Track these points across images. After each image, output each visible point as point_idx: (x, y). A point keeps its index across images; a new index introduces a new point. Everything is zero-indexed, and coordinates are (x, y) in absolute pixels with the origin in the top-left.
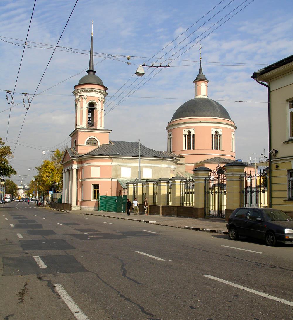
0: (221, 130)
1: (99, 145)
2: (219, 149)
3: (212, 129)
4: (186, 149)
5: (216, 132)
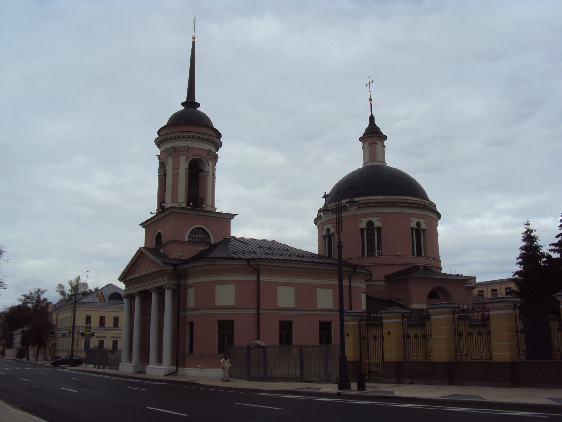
0: (424, 220)
1: (213, 241)
3: (411, 219)
4: (366, 255)
5: (418, 224)
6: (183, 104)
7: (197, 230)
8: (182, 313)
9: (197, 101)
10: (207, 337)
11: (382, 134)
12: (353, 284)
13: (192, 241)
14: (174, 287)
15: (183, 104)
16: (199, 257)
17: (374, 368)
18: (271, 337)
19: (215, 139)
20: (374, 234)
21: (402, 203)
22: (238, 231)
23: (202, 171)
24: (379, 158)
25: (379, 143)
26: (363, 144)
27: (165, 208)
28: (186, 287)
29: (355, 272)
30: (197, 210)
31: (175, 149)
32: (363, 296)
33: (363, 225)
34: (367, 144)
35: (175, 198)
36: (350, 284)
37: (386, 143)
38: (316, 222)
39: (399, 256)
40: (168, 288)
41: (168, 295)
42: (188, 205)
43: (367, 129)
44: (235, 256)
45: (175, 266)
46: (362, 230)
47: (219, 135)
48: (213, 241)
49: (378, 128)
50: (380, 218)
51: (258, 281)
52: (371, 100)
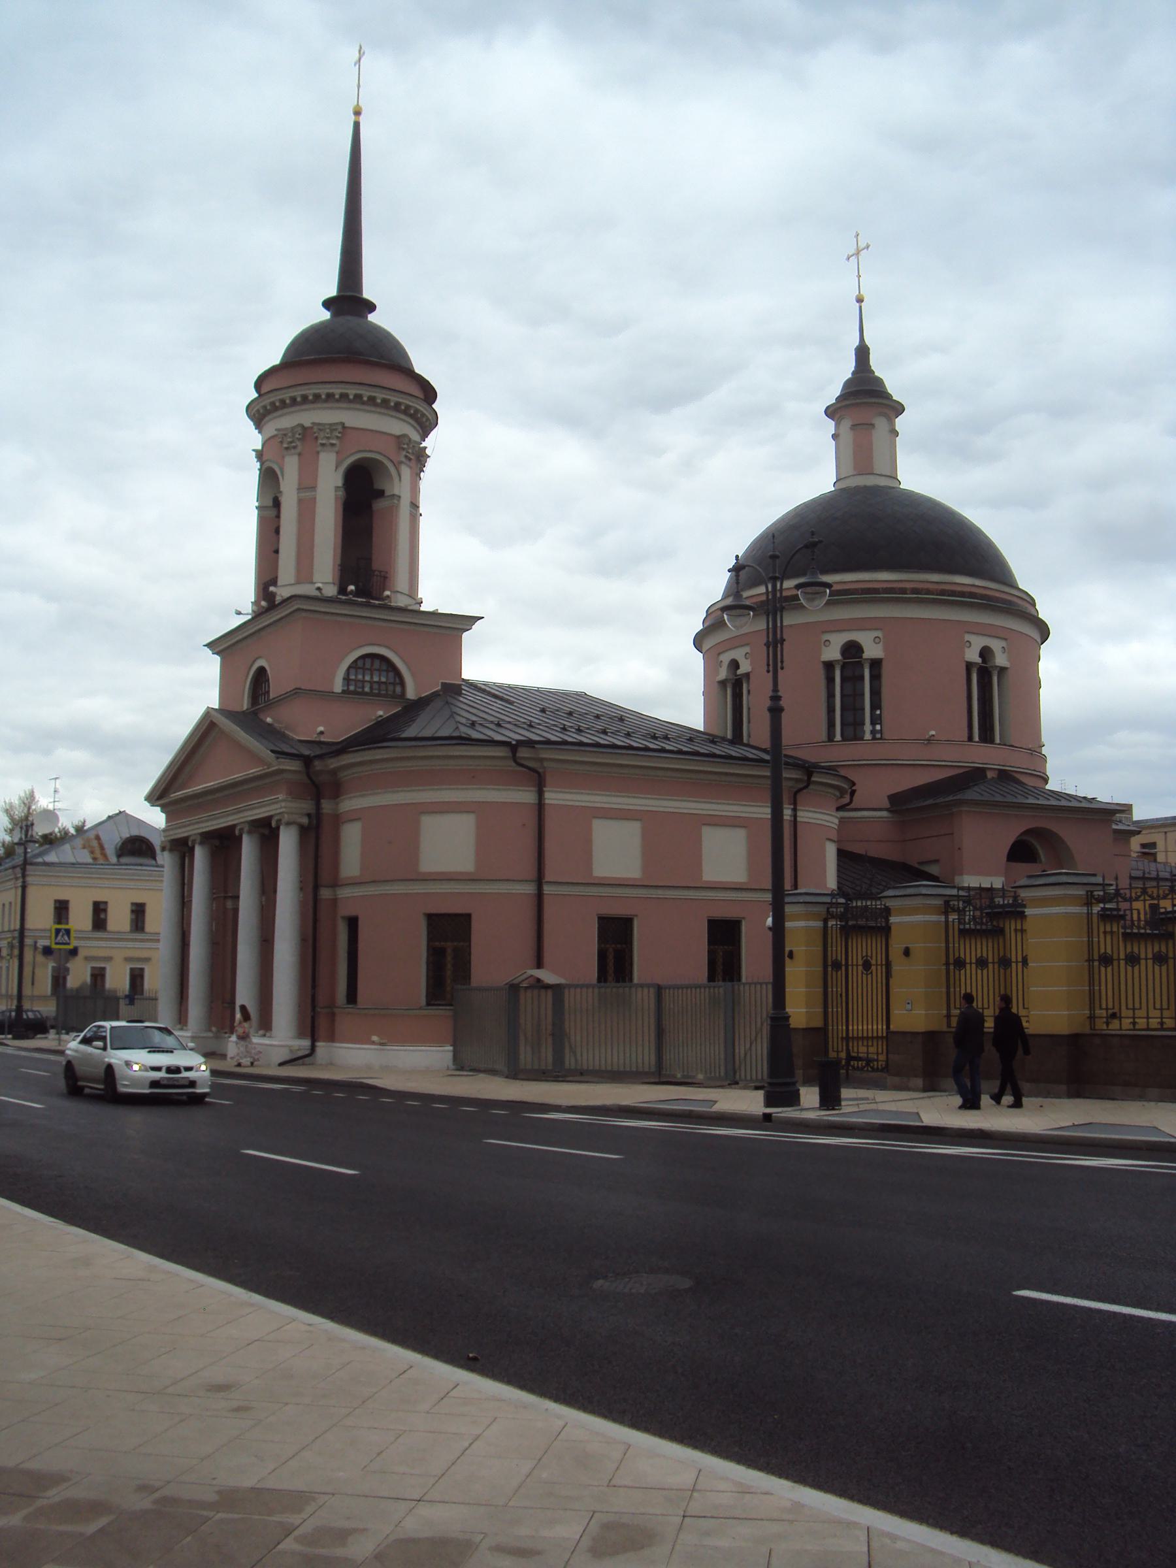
0: (1004, 644)
1: (411, 694)
3: (967, 637)
4: (838, 737)
5: (985, 653)
6: (327, 304)
7: (368, 661)
8: (325, 893)
9: (367, 294)
10: (396, 960)
11: (888, 397)
12: (804, 816)
13: (355, 693)
14: (305, 821)
15: (327, 304)
16: (375, 736)
17: (863, 1049)
18: (573, 957)
19: (418, 402)
20: (862, 678)
21: (943, 592)
22: (479, 664)
23: (381, 494)
24: (880, 466)
25: (881, 423)
26: (837, 426)
27: (278, 599)
28: (338, 820)
29: (809, 783)
30: (367, 605)
31: (305, 433)
32: (831, 851)
33: (833, 653)
34: (846, 424)
35: (304, 571)
36: (795, 816)
37: (900, 422)
38: (699, 641)
39: (930, 740)
40: (288, 824)
41: (288, 842)
42: (342, 590)
43: (848, 384)
44: (475, 735)
45: (307, 761)
46: (829, 666)
47: (429, 393)
48: (411, 694)
49: (879, 381)
50: (879, 634)
51: (541, 806)
52: (860, 300)
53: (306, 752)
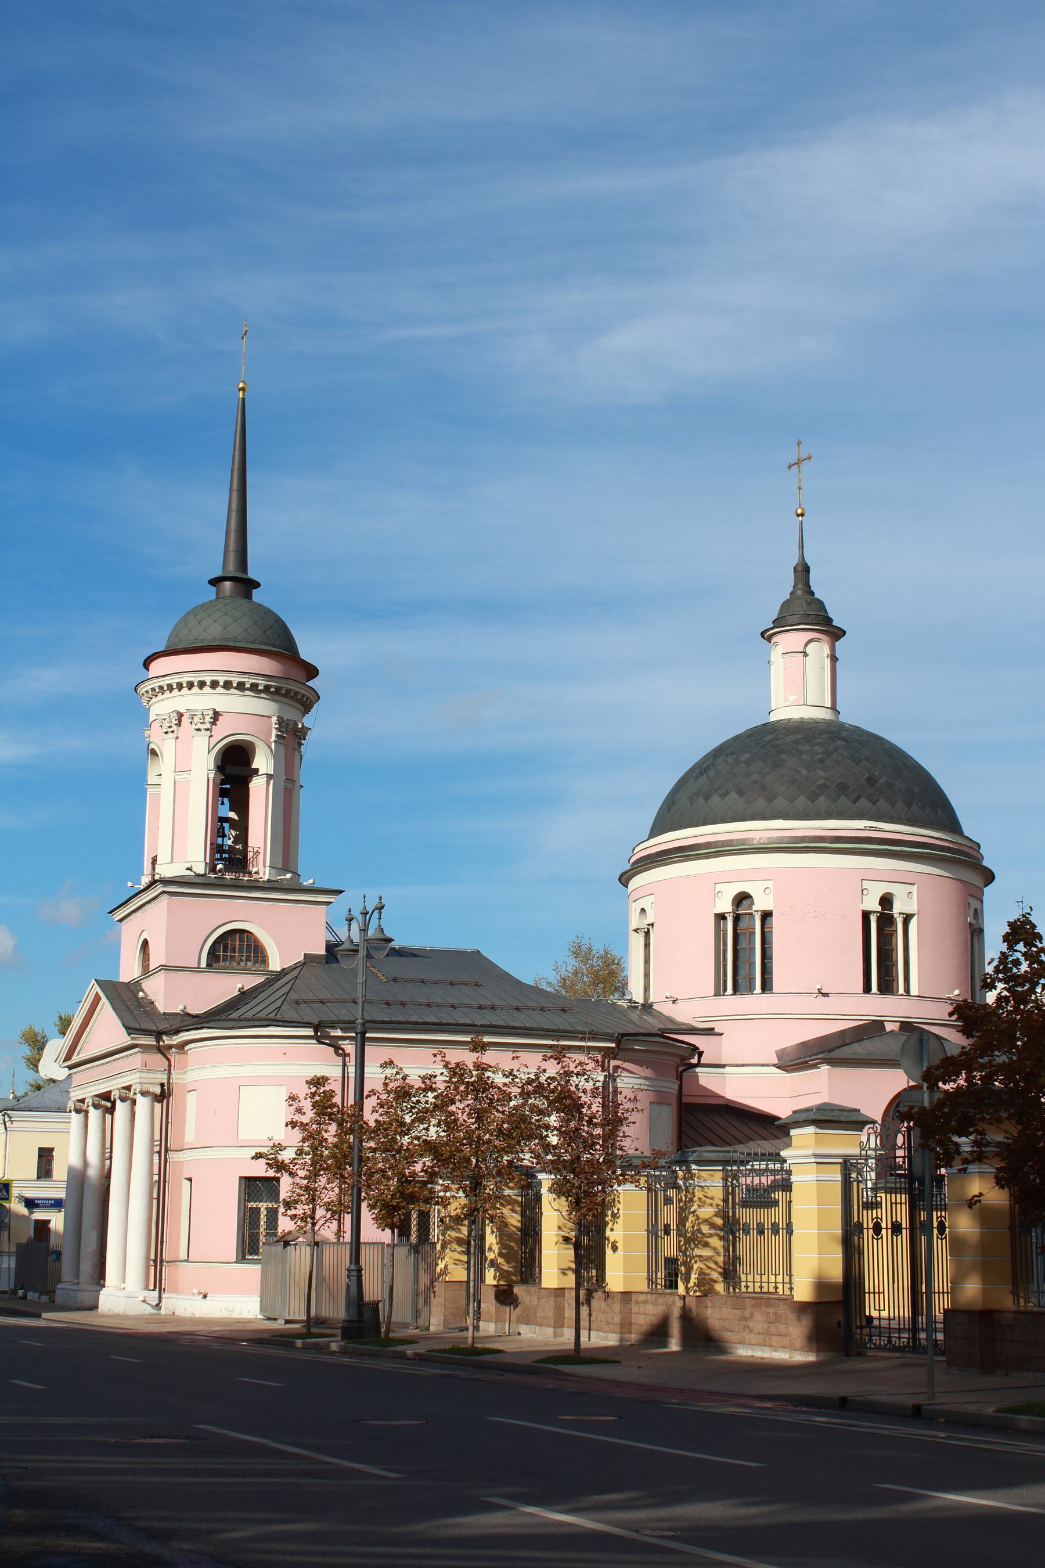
1: (275, 964)
2: (901, 991)
5: (886, 901)
8: (173, 1157)
33: (725, 906)
46: (721, 917)
50: (770, 884)
53: (162, 1027)
